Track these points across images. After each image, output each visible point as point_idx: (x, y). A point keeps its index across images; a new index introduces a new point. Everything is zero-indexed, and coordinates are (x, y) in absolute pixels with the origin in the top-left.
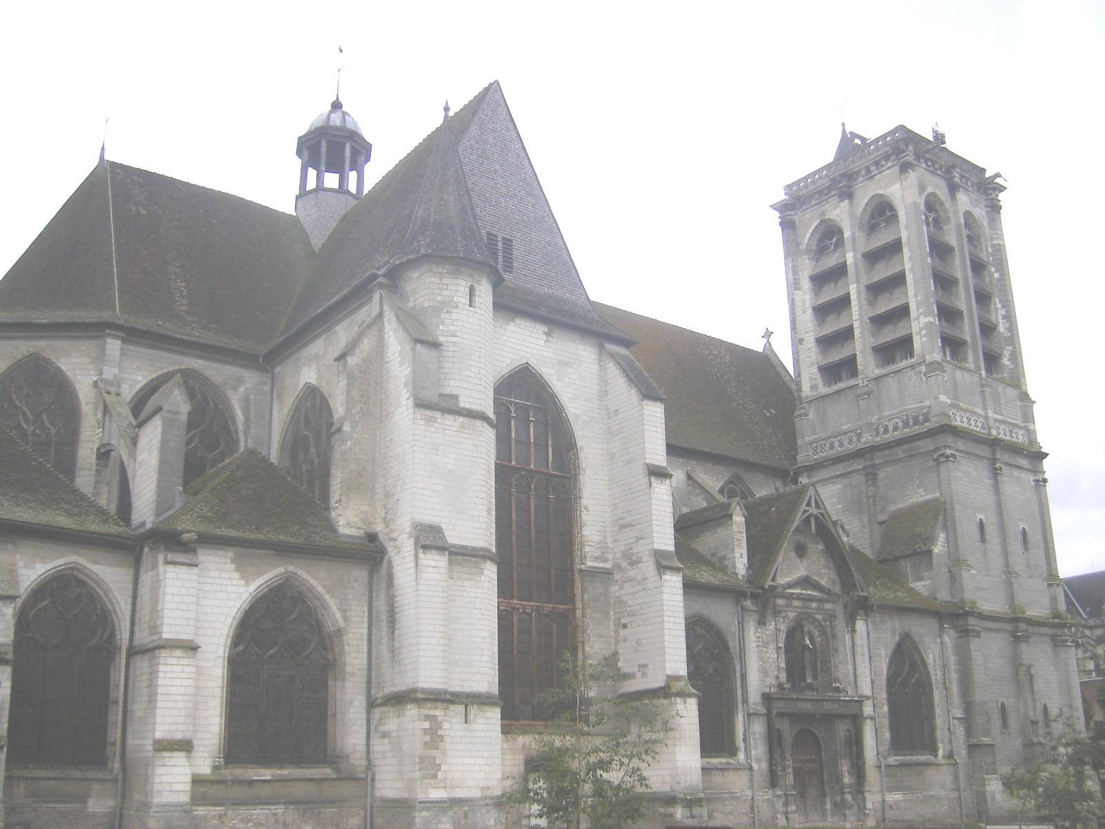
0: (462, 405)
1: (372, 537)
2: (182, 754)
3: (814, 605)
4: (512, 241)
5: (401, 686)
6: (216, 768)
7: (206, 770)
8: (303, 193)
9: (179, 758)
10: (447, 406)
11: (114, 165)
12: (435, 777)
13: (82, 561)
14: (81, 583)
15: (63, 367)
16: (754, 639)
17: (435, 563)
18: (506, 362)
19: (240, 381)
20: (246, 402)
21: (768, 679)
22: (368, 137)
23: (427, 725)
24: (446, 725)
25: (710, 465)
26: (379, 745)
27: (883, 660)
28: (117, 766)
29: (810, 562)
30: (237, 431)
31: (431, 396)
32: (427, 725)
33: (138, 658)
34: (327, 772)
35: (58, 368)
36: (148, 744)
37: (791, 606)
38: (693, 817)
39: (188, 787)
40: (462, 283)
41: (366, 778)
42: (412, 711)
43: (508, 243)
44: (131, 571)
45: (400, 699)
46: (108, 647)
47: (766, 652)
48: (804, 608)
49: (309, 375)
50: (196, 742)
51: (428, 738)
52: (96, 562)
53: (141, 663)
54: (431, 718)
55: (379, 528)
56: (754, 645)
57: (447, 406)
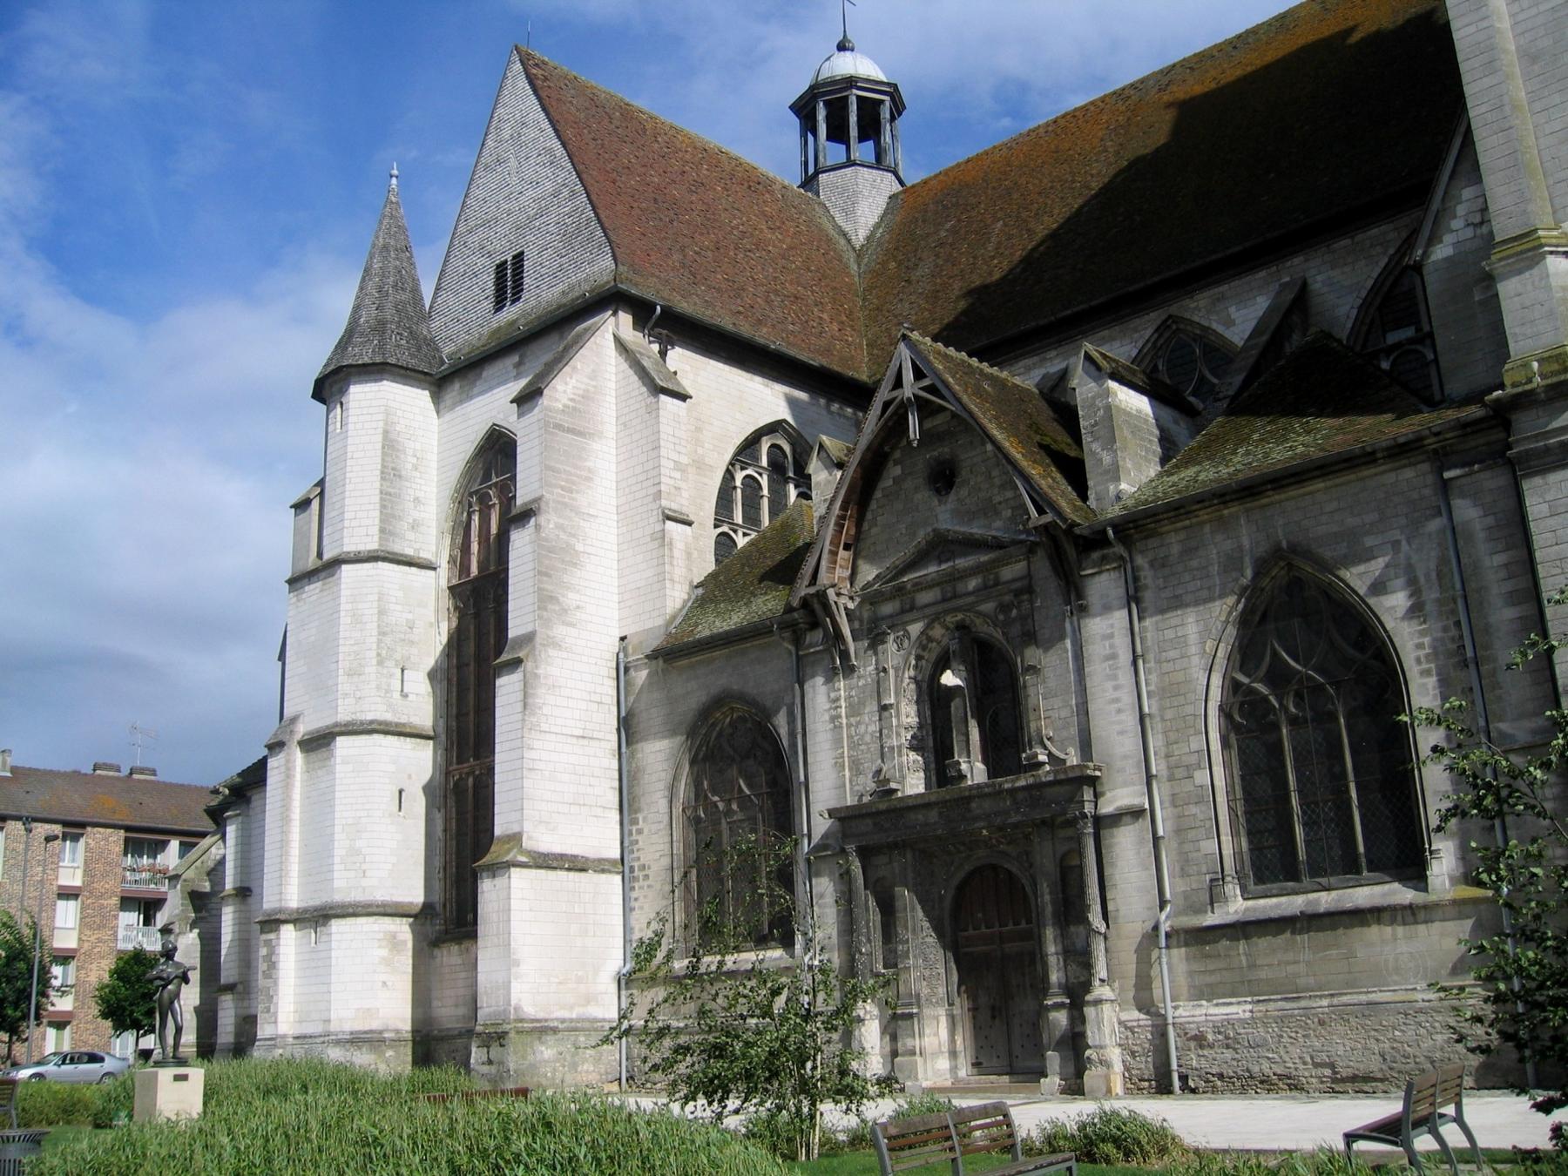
3: (973, 584)
16: (827, 706)
21: (861, 779)
25: (1347, 242)
27: (1193, 650)
29: (964, 492)
37: (912, 609)
38: (490, 1062)
47: (859, 723)
48: (944, 600)
56: (827, 717)
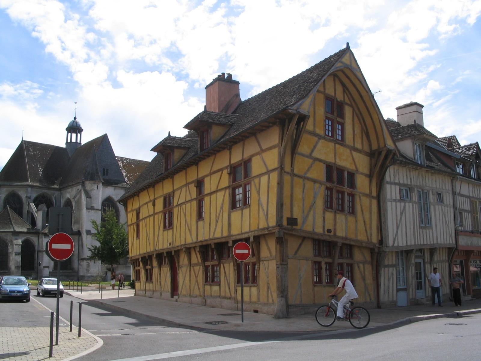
0: (95, 208)
1: (79, 231)
2: (48, 268)
4: (108, 169)
5: (83, 257)
6: (53, 271)
7: (51, 271)
8: (67, 143)
9: (47, 269)
10: (92, 208)
11: (25, 141)
12: (88, 272)
13: (30, 237)
14: (30, 241)
15: (19, 193)
17: (89, 237)
18: (106, 196)
19: (54, 194)
20: (55, 198)
22: (83, 127)
23: (87, 264)
24: (91, 264)
26: (80, 267)
28: (36, 270)
30: (54, 204)
31: (90, 207)
32: (87, 264)
33: (39, 253)
34: (71, 271)
35: (18, 194)
36: (42, 267)
39: (49, 273)
40: (96, 185)
41: (78, 272)
42: (85, 261)
43: (107, 170)
44: (37, 238)
45: (83, 259)
46: (34, 250)
49: (68, 196)
50: (50, 266)
51: (87, 266)
52: (32, 237)
53: (40, 254)
54: (88, 263)
55: (80, 229)
57: (92, 208)
